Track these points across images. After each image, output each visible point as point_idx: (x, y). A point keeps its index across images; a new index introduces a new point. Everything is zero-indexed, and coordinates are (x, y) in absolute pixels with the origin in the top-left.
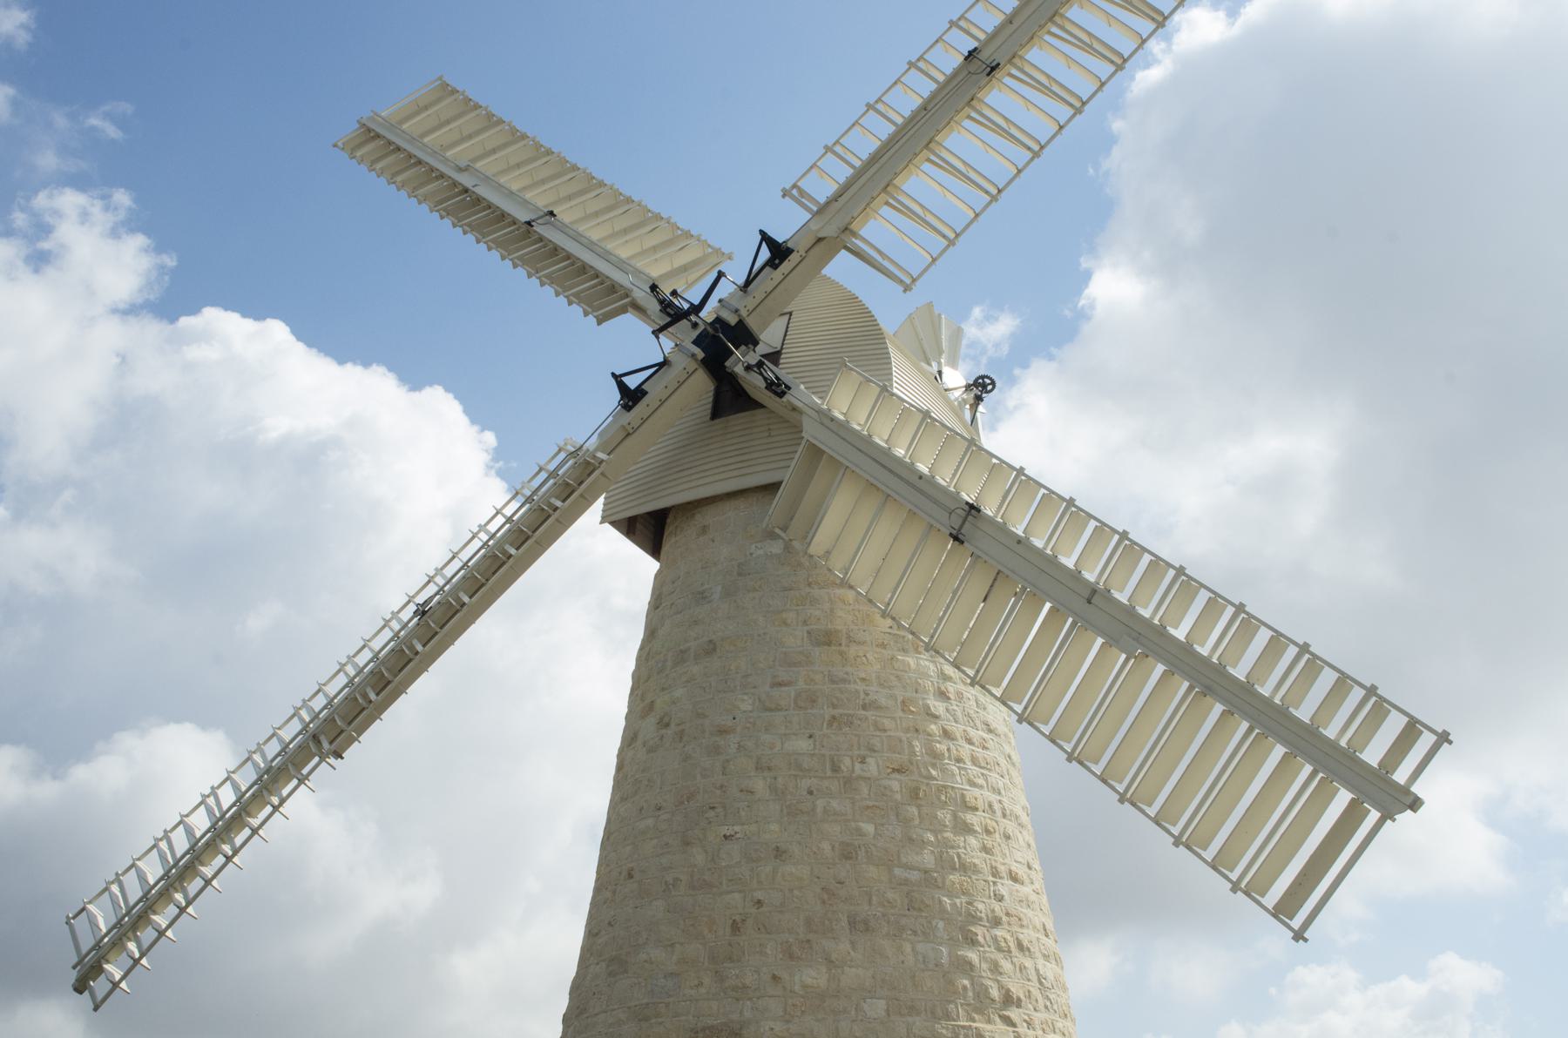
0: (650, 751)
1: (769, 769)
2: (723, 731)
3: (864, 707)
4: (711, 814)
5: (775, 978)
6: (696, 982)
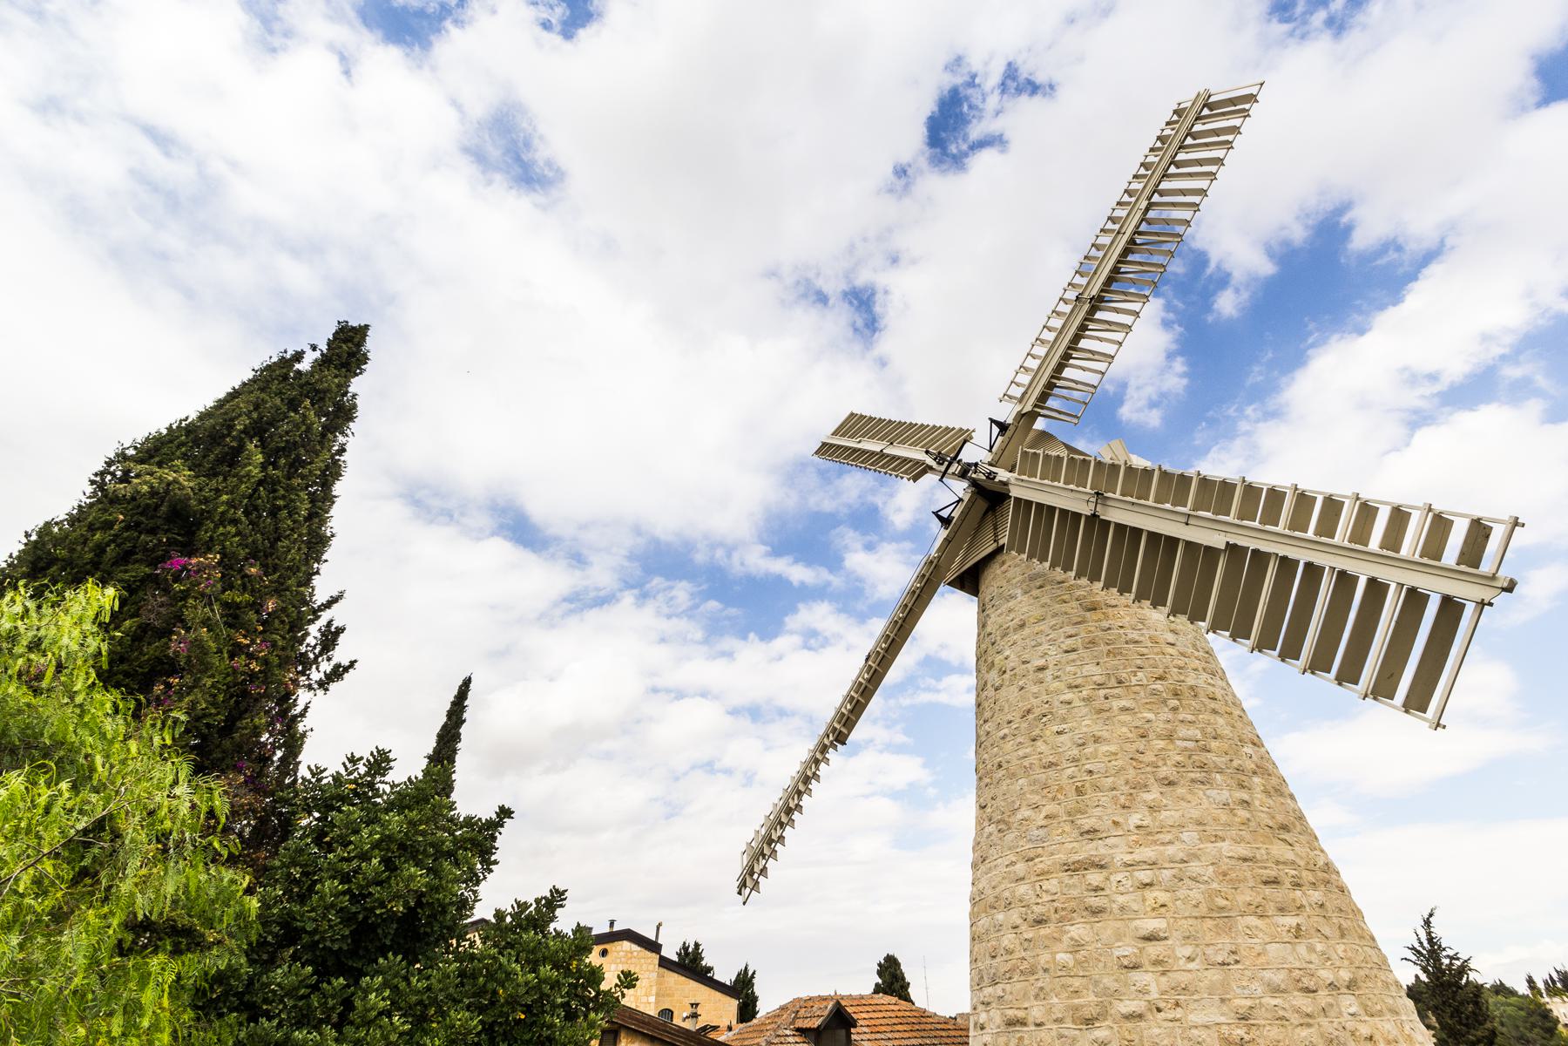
0: (996, 690)
1: (1076, 687)
2: (1042, 669)
3: (1127, 643)
4: (1045, 719)
5: (1116, 823)
6: (1060, 831)
